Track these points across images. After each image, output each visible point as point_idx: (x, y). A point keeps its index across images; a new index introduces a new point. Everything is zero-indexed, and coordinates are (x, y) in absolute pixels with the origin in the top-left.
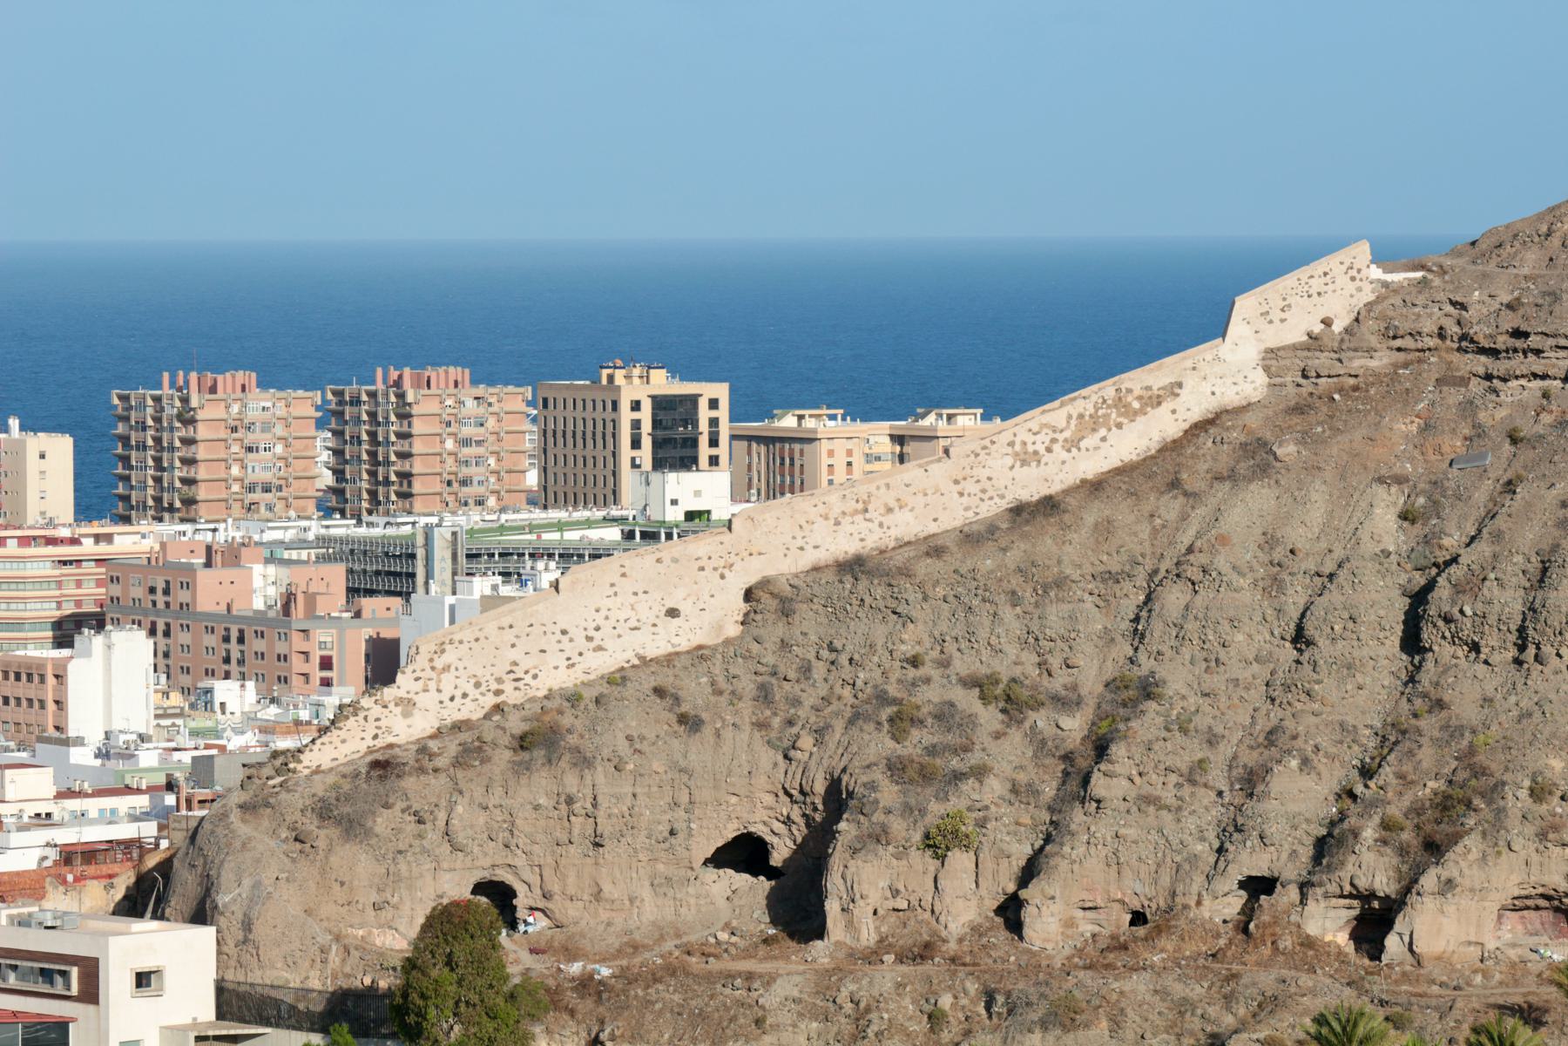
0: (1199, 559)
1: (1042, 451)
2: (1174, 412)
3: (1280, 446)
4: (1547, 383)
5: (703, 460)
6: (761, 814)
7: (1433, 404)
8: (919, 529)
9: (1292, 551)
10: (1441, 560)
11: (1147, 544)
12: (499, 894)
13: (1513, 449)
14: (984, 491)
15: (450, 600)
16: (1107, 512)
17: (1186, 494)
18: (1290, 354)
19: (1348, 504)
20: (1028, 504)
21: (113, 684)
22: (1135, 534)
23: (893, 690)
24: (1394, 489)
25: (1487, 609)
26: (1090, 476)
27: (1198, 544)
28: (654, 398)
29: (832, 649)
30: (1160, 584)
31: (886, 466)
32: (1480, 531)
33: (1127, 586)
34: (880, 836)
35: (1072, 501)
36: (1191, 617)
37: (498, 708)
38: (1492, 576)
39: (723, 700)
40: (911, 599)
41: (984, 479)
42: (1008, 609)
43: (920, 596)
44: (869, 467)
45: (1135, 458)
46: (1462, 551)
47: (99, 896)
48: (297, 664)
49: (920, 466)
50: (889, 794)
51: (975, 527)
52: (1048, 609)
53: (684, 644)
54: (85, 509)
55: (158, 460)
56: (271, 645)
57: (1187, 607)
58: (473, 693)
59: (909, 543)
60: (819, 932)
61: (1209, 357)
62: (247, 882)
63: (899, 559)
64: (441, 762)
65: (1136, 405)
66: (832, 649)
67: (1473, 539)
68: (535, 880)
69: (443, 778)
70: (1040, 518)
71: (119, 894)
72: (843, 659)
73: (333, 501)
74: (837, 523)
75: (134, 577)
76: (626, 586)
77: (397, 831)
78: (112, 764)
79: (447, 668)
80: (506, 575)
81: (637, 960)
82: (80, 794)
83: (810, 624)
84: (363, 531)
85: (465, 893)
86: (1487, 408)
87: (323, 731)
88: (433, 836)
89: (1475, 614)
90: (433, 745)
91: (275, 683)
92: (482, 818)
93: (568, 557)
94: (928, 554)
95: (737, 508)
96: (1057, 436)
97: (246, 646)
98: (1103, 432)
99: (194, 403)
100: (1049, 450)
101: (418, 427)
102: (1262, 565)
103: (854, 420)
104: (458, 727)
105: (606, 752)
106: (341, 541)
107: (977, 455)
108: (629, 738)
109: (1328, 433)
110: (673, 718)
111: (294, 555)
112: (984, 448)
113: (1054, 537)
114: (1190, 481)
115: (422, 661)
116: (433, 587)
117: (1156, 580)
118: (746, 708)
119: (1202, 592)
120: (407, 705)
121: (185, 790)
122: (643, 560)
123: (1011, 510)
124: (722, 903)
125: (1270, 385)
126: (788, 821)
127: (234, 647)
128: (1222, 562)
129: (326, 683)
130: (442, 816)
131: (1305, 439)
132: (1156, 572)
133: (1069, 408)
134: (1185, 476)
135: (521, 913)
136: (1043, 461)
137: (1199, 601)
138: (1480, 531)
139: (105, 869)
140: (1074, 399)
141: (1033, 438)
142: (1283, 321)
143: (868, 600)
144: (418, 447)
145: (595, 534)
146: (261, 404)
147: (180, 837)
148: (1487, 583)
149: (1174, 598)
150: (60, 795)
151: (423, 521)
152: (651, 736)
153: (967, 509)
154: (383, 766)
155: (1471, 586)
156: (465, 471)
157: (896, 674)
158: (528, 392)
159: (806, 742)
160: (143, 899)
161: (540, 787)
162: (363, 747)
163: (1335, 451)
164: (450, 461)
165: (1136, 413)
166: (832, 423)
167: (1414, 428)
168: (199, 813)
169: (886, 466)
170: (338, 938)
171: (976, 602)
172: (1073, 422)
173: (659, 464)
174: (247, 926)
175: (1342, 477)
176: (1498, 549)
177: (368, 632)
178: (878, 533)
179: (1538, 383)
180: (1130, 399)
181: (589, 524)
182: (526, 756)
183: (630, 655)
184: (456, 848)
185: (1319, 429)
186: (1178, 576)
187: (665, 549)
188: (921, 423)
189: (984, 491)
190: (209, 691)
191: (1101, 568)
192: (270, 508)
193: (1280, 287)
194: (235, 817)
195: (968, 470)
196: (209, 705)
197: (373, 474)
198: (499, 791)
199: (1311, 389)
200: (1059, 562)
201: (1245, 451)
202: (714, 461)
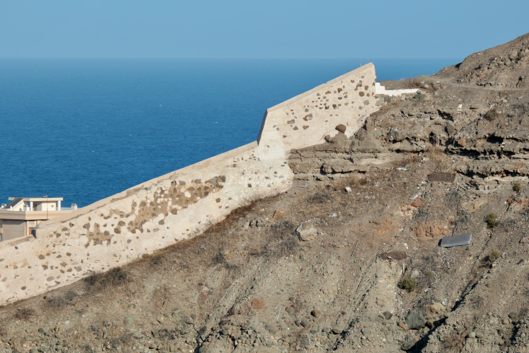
2: (218, 200)
3: (303, 228)
4: (517, 178)
7: (425, 195)
8: (10, 295)
9: (313, 314)
10: (432, 321)
11: (196, 307)
13: (489, 231)
14: (64, 265)
16: (164, 282)
17: (228, 267)
18: (311, 154)
19: (357, 275)
20: (100, 275)
22: (187, 299)
24: (394, 263)
26: (150, 252)
27: (237, 307)
30: (207, 340)
32: (463, 298)
33: (180, 341)
38: (473, 334)
41: (64, 254)
45: (186, 237)
46: (448, 314)
49: (12, 244)
51: (56, 294)
61: (246, 157)
65: (188, 195)
67: (457, 304)
70: (109, 287)
86: (468, 199)
94: (17, 316)
96: (124, 219)
98: (161, 216)
100: (117, 231)
102: (289, 324)
107: (58, 235)
109: (341, 218)
112: (65, 229)
113: (121, 302)
114: (232, 256)
117: (204, 337)
119: (240, 346)
123: (86, 280)
128: (257, 322)
131: (323, 222)
132: (203, 330)
134: (227, 252)
136: (112, 240)
138: (463, 298)
140: (138, 190)
141: (104, 222)
142: (305, 127)
148: (469, 340)
153: (50, 279)
163: (347, 232)
165: (188, 201)
167: (410, 214)
172: (137, 209)
175: (353, 254)
176: (477, 312)
179: (509, 179)
180: (183, 190)
185: (335, 215)
186: (221, 333)
188: (12, 209)
189: (64, 265)
191: (159, 327)
195: (51, 248)
199: (327, 182)
200: (125, 322)
201: (276, 232)
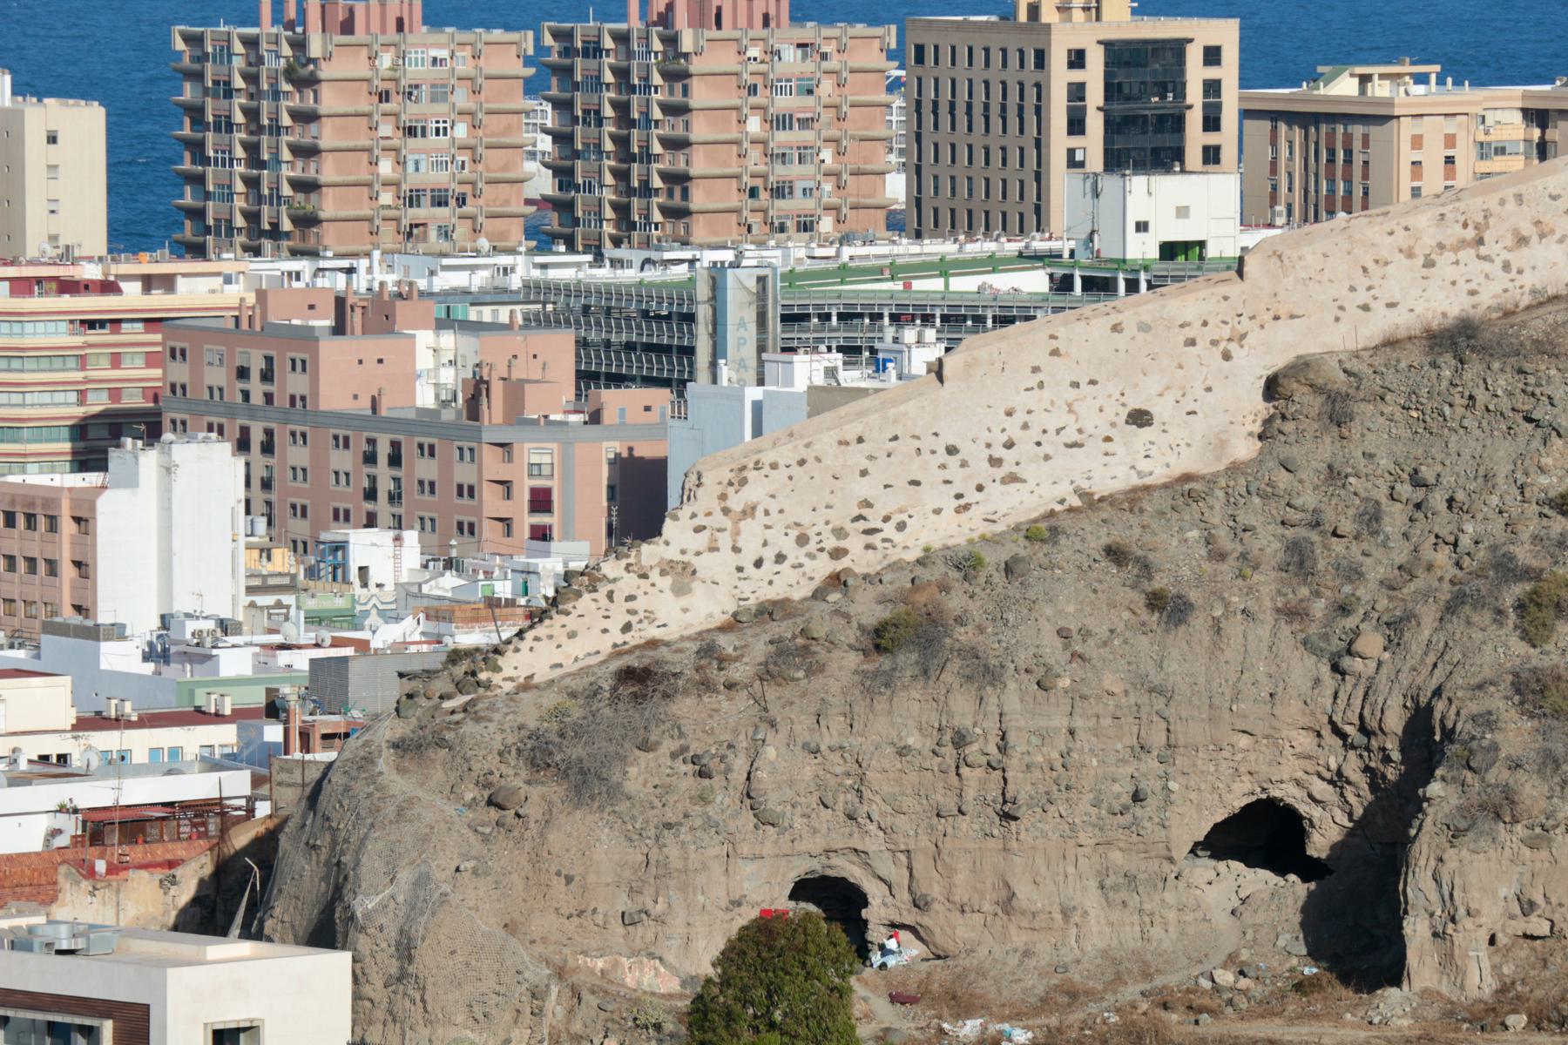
5: (1193, 155)
6: (1291, 767)
12: (837, 899)
15: (754, 393)
21: (174, 535)
23: (1524, 554)
28: (1108, 45)
29: (1417, 481)
31: (1515, 163)
34: (1500, 808)
37: (837, 581)
39: (1227, 569)
44: (1484, 166)
47: (151, 895)
48: (491, 502)
50: (1516, 734)
53: (1159, 471)
54: (127, 234)
55: (252, 149)
56: (446, 469)
58: (794, 554)
59: (1555, 298)
60: (1394, 974)
62: (405, 876)
63: (1538, 326)
64: (739, 672)
66: (1417, 481)
68: (899, 876)
69: (742, 701)
71: (185, 892)
72: (1438, 500)
73: (553, 221)
75: (211, 351)
76: (1059, 372)
77: (663, 790)
78: (172, 671)
79: (749, 511)
80: (850, 351)
81: (1076, 1017)
82: (118, 723)
83: (1379, 438)
84: (604, 274)
85: (782, 902)
87: (537, 616)
88: (724, 799)
90: (726, 643)
91: (454, 533)
92: (808, 769)
93: (958, 321)
95: (1253, 238)
97: (397, 469)
99: (315, 50)
101: (700, 94)
103: (1458, 83)
104: (768, 611)
105: (1023, 658)
106: (567, 290)
108: (1063, 634)
110: (1140, 600)
111: (486, 314)
115: (707, 498)
116: (725, 372)
118: (1266, 582)
120: (682, 574)
121: (299, 717)
122: (1088, 329)
124: (1222, 920)
126: (1338, 780)
127: (383, 470)
129: (541, 534)
130: (740, 764)
135: (875, 934)
139: (160, 852)
143: (1482, 397)
144: (700, 129)
145: (1003, 282)
146: (431, 52)
147: (290, 798)
150: (84, 724)
151: (708, 257)
152: (1101, 630)
154: (640, 678)
156: (780, 172)
157: (1531, 527)
158: (891, 35)
159: (1372, 643)
160: (227, 904)
161: (908, 716)
162: (605, 645)
164: (755, 154)
166: (1420, 89)
168: (324, 756)
169: (1515, 163)
170: (561, 973)
173: (1115, 161)
174: (405, 950)
177: (613, 447)
178: (1501, 281)
181: (993, 264)
182: (885, 662)
183: (1064, 490)
184: (764, 820)
187: (1130, 309)
190: (340, 547)
192: (445, 233)
194: (385, 764)
196: (339, 571)
197: (622, 176)
198: (837, 723)
202: (1212, 155)
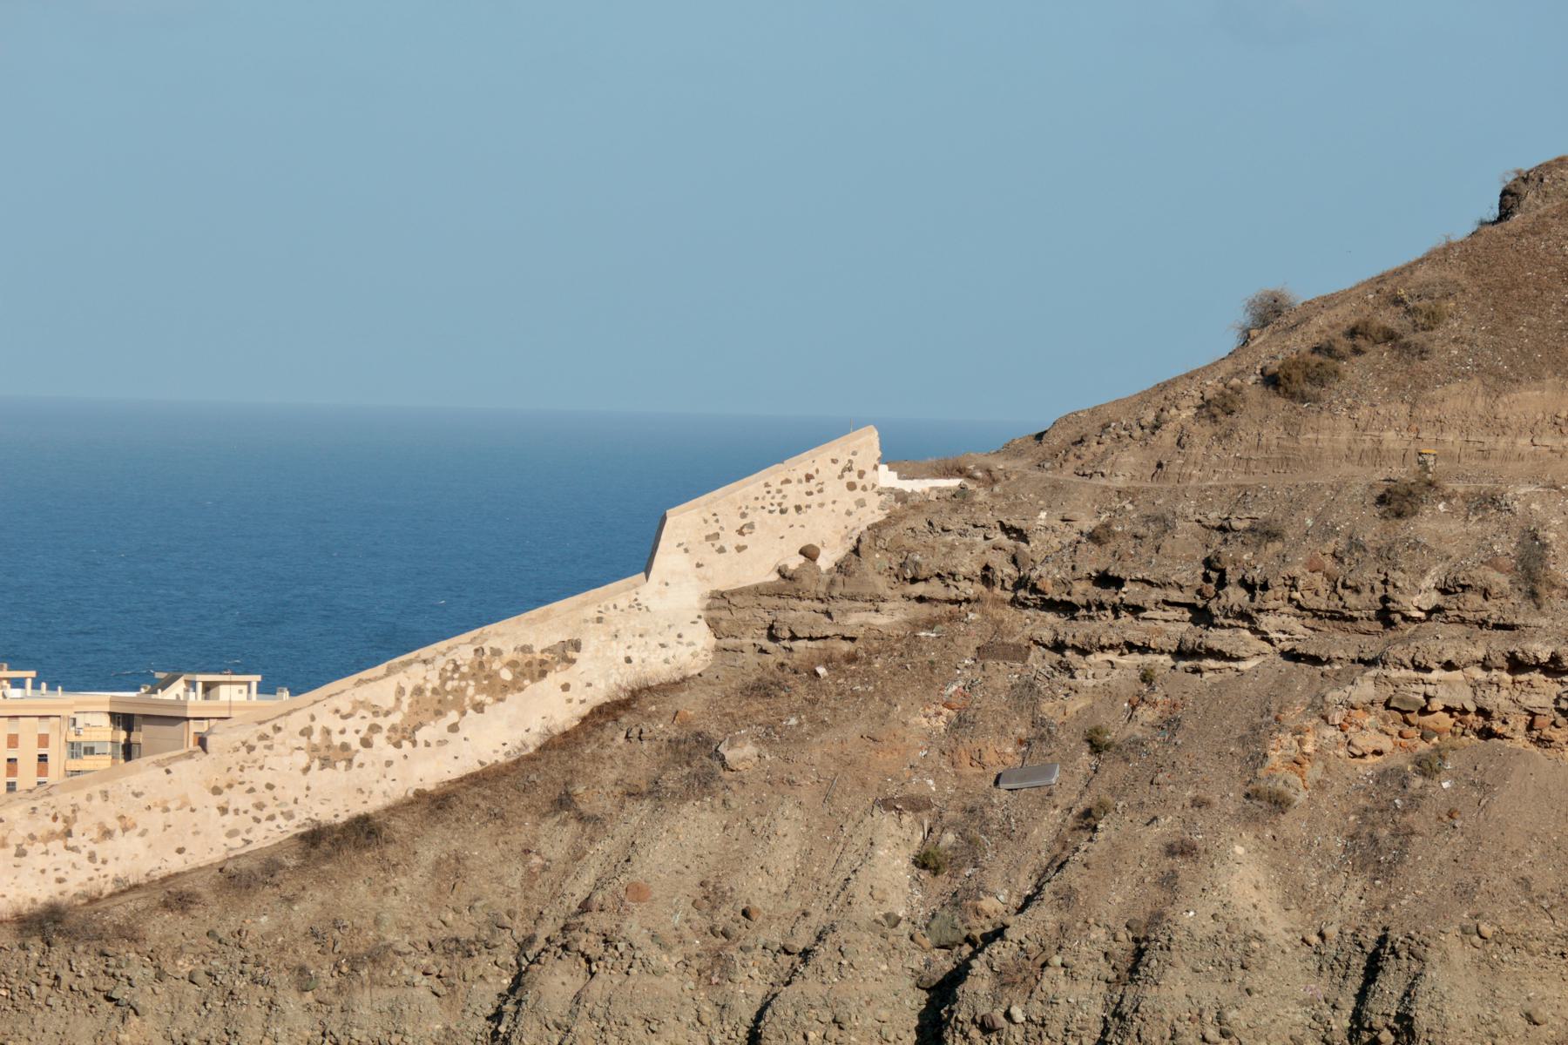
0: (598, 921)
1: (355, 743)
2: (566, 687)
3: (732, 746)
4: (1149, 658)
7: (971, 686)
8: (154, 864)
9: (745, 913)
10: (977, 933)
11: (518, 896)
13: (1093, 760)
14: (260, 806)
16: (455, 844)
17: (581, 818)
18: (751, 601)
19: (835, 841)
20: (331, 828)
22: (500, 880)
24: (907, 819)
25: (1049, 1012)
26: (429, 786)
27: (598, 897)
30: (537, 960)
31: (103, 762)
32: (1039, 888)
33: (483, 962)
35: (400, 825)
36: (583, 1014)
38: (1057, 960)
40: (137, 975)
41: (260, 786)
42: (292, 995)
43: (151, 972)
44: (75, 764)
45: (501, 759)
46: (1011, 920)
49: (159, 764)
51: (244, 864)
52: (357, 996)
57: (577, 999)
59: (136, 887)
61: (623, 603)
63: (119, 912)
65: (507, 675)
67: (1028, 900)
70: (348, 852)
74: (21, 853)
86: (1054, 695)
89: (1029, 1020)
94: (166, 905)
96: (379, 721)
98: (453, 716)
100: (366, 743)
102: (699, 933)
107: (251, 749)
109: (806, 727)
112: (263, 737)
113: (370, 882)
114: (590, 798)
117: (531, 954)
119: (602, 974)
123: (302, 837)
125: (717, 649)
128: (635, 928)
131: (770, 735)
132: (530, 940)
133: (400, 678)
134: (580, 790)
136: (356, 761)
137: (596, 987)
138: (1039, 888)
140: (409, 663)
141: (341, 724)
142: (740, 549)
143: (66, 977)
148: (1049, 971)
149: (557, 983)
153: (232, 834)
155: (1025, 975)
163: (817, 755)
165: (506, 688)
166: (17, 692)
167: (941, 723)
171: (240, 984)
172: (406, 700)
175: (827, 798)
176: (1066, 917)
178: (87, 870)
179: (1135, 659)
180: (496, 666)
185: (793, 721)
186: (565, 947)
188: (161, 695)
189: (260, 806)
191: (443, 933)
193: (738, 495)
195: (236, 773)
199: (781, 657)
200: (377, 922)
201: (677, 752)
